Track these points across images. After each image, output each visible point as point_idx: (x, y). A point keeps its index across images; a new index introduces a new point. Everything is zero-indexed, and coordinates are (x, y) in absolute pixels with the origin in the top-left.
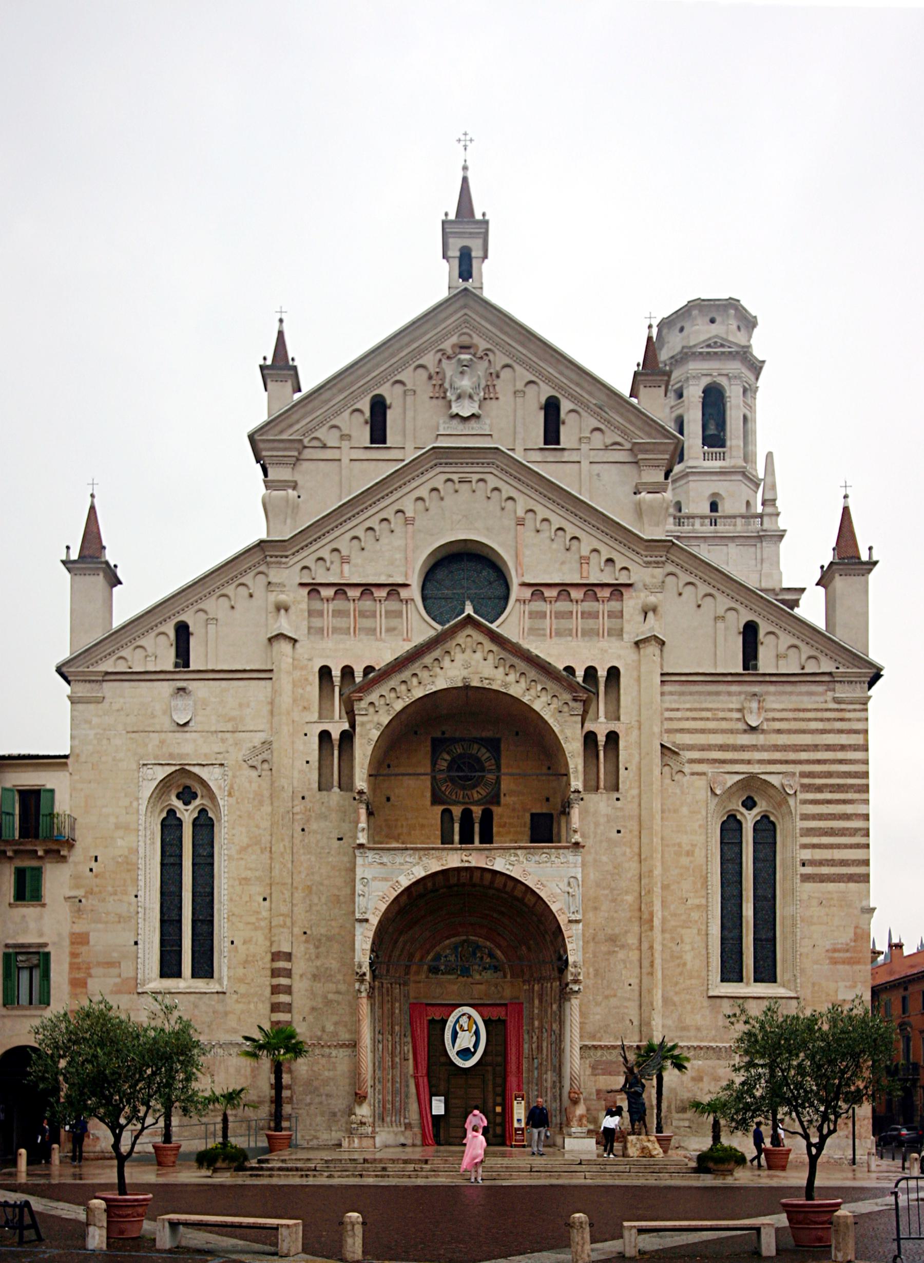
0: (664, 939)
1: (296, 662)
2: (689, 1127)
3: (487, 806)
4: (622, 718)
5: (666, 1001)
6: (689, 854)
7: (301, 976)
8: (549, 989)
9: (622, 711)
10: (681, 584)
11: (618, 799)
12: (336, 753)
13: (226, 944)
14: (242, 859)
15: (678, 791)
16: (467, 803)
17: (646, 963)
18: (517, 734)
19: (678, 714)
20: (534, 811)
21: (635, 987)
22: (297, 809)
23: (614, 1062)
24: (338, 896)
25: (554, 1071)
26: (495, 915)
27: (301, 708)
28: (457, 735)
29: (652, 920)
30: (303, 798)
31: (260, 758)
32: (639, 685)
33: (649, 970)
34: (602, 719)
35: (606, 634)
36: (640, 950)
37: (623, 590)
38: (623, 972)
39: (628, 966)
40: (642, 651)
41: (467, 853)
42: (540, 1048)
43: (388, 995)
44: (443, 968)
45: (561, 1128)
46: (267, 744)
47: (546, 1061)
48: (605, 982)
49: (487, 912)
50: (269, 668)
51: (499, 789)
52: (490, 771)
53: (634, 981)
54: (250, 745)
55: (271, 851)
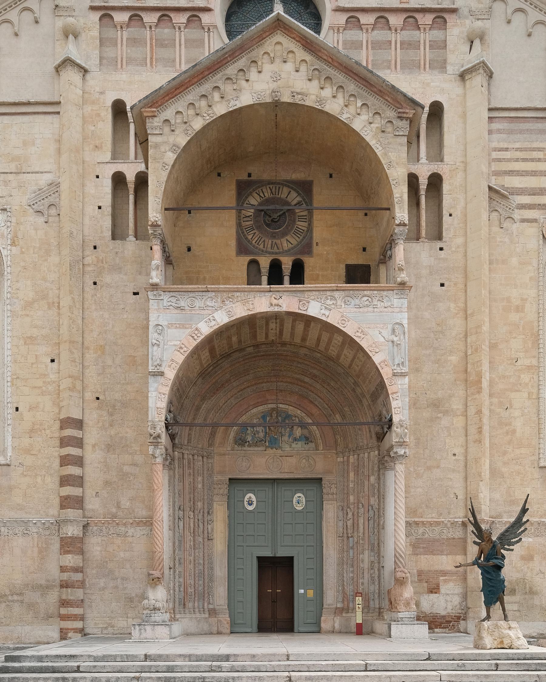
0: (491, 404)
1: (86, 95)
2: (519, 611)
3: (299, 257)
4: (446, 158)
5: (494, 472)
6: (519, 309)
7: (94, 446)
8: (366, 460)
9: (446, 151)
10: (509, 11)
11: (441, 249)
12: (132, 198)
13: (10, 411)
14: (28, 315)
15: (507, 240)
16: (276, 253)
17: (472, 430)
18: (331, 176)
19: (508, 155)
20: (350, 262)
21: (462, 458)
22: (88, 260)
23: (438, 540)
24: (134, 357)
25: (372, 550)
26: (307, 379)
27: (91, 146)
28: (265, 177)
29: (479, 382)
30: (95, 247)
31: (47, 202)
32: (465, 123)
33: (477, 437)
34: (423, 160)
35: (427, 66)
36: (466, 416)
37: (446, 16)
38: (447, 441)
39: (452, 434)
40: (468, 83)
41: (278, 295)
42: (355, 525)
43: (189, 467)
44: (249, 438)
45: (380, 613)
46: (55, 186)
47: (363, 540)
48: (427, 451)
49: (298, 376)
50: (56, 99)
51: (311, 238)
52: (301, 218)
53: (459, 450)
54: (35, 188)
55: (59, 307)
